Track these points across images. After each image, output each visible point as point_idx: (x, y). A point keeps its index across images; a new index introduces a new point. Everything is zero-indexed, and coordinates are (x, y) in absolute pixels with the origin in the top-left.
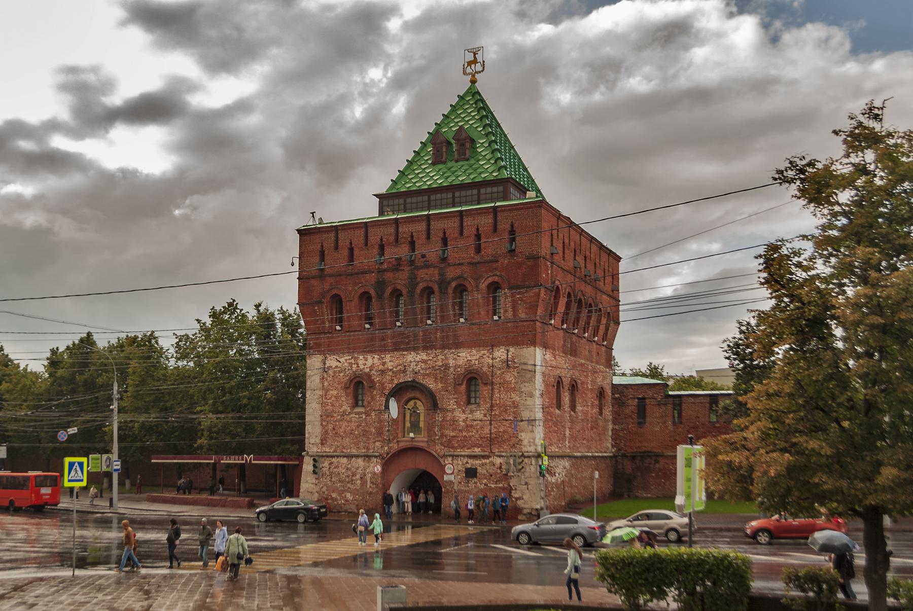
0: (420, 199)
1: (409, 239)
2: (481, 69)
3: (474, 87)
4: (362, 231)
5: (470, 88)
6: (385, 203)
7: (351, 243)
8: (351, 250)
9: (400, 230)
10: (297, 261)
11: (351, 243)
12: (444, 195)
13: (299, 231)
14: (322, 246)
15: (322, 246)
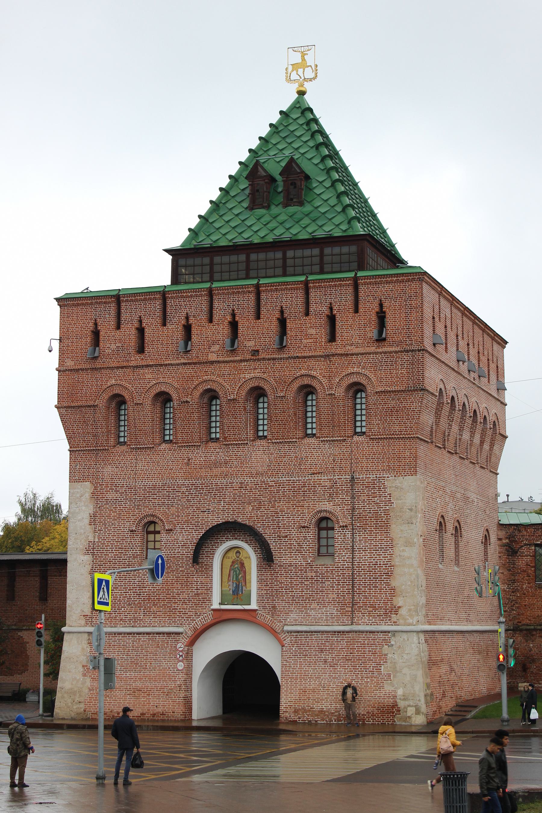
0: (234, 258)
1: (229, 318)
2: (312, 75)
3: (304, 101)
4: (158, 304)
5: (297, 101)
6: (182, 262)
7: (140, 321)
8: (141, 331)
9: (216, 304)
10: (56, 345)
11: (140, 321)
12: (271, 255)
13: (58, 300)
14: (96, 324)
15: (96, 324)
